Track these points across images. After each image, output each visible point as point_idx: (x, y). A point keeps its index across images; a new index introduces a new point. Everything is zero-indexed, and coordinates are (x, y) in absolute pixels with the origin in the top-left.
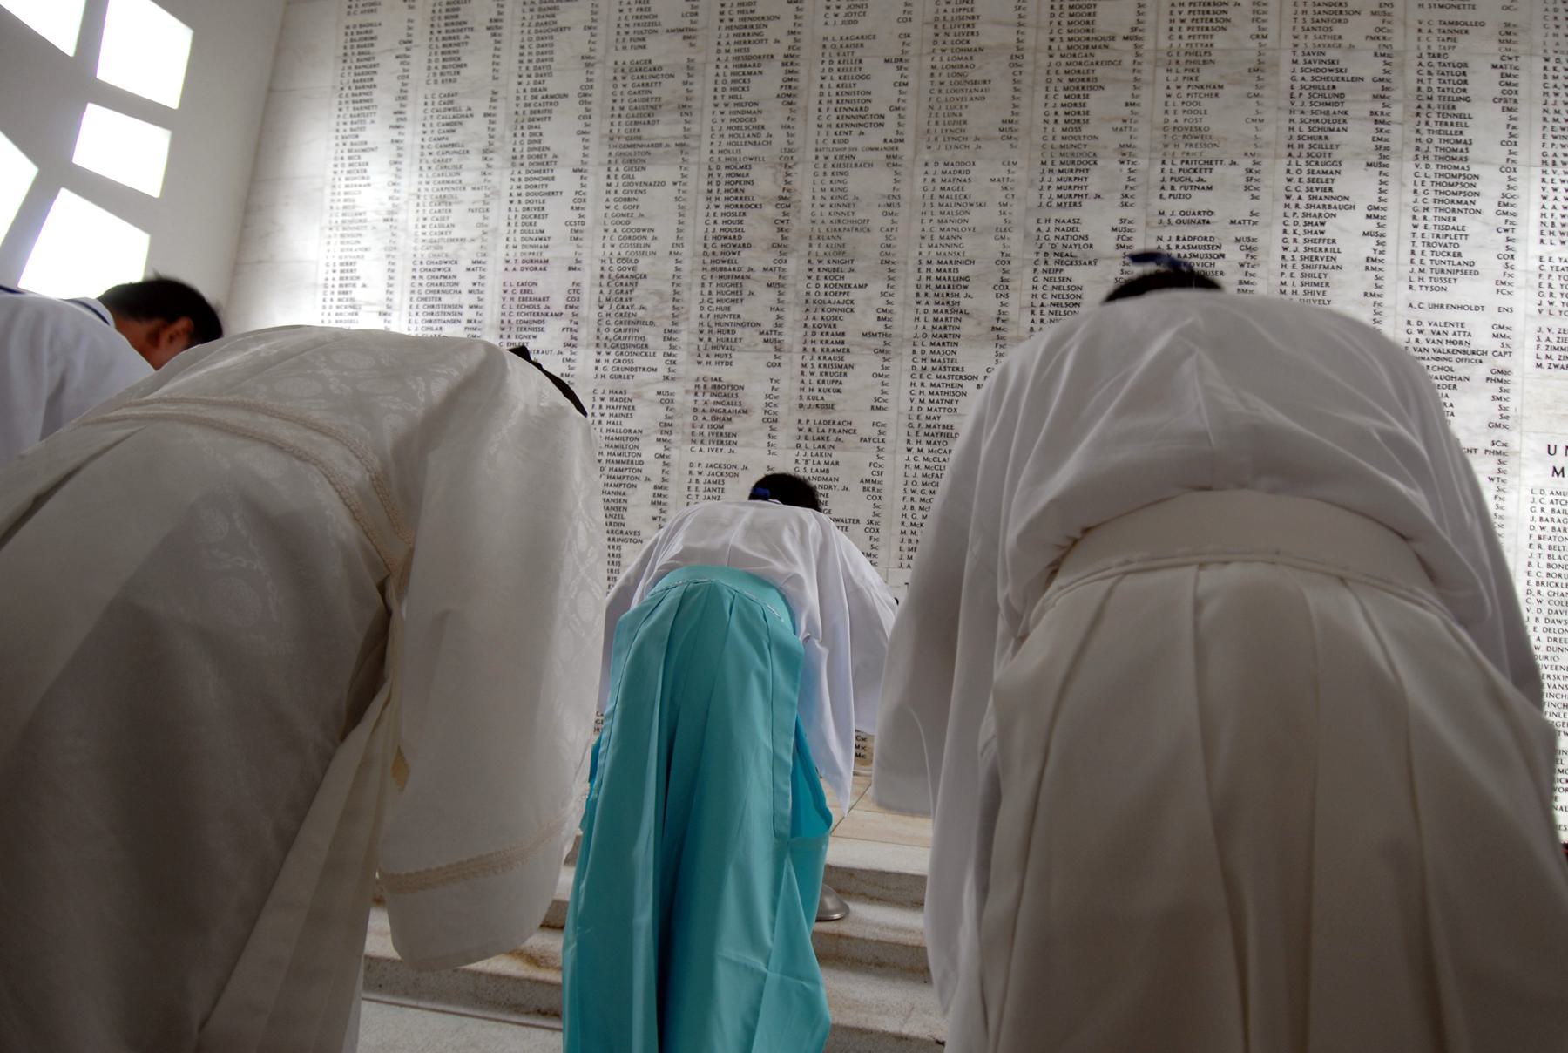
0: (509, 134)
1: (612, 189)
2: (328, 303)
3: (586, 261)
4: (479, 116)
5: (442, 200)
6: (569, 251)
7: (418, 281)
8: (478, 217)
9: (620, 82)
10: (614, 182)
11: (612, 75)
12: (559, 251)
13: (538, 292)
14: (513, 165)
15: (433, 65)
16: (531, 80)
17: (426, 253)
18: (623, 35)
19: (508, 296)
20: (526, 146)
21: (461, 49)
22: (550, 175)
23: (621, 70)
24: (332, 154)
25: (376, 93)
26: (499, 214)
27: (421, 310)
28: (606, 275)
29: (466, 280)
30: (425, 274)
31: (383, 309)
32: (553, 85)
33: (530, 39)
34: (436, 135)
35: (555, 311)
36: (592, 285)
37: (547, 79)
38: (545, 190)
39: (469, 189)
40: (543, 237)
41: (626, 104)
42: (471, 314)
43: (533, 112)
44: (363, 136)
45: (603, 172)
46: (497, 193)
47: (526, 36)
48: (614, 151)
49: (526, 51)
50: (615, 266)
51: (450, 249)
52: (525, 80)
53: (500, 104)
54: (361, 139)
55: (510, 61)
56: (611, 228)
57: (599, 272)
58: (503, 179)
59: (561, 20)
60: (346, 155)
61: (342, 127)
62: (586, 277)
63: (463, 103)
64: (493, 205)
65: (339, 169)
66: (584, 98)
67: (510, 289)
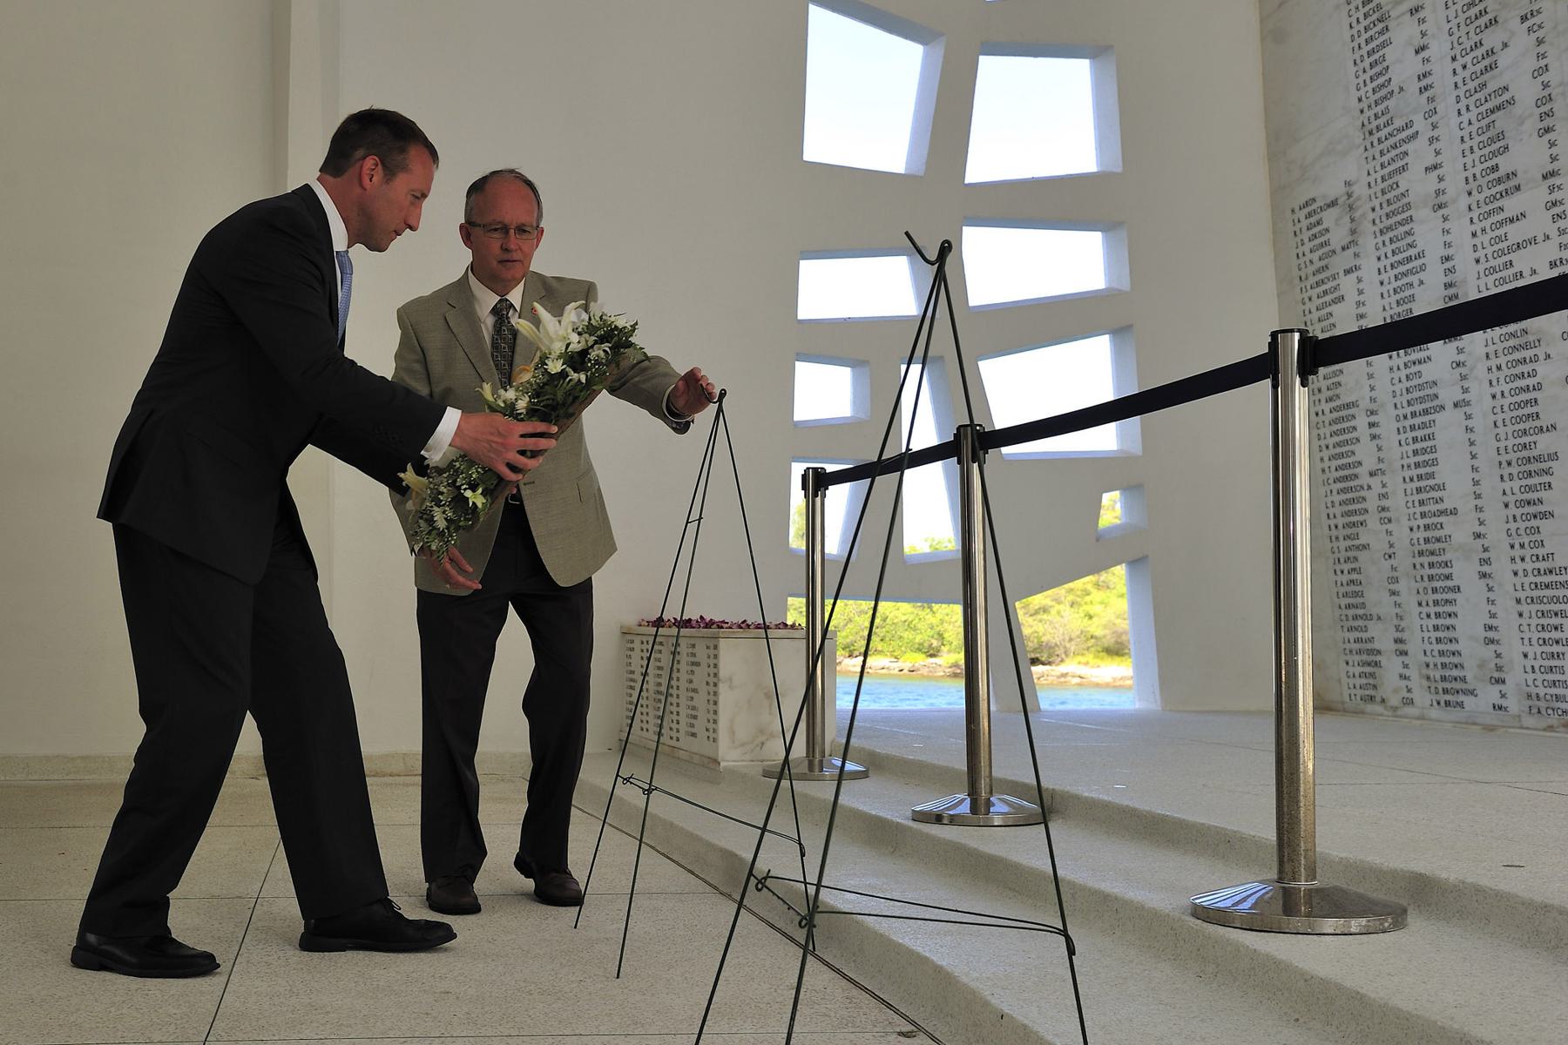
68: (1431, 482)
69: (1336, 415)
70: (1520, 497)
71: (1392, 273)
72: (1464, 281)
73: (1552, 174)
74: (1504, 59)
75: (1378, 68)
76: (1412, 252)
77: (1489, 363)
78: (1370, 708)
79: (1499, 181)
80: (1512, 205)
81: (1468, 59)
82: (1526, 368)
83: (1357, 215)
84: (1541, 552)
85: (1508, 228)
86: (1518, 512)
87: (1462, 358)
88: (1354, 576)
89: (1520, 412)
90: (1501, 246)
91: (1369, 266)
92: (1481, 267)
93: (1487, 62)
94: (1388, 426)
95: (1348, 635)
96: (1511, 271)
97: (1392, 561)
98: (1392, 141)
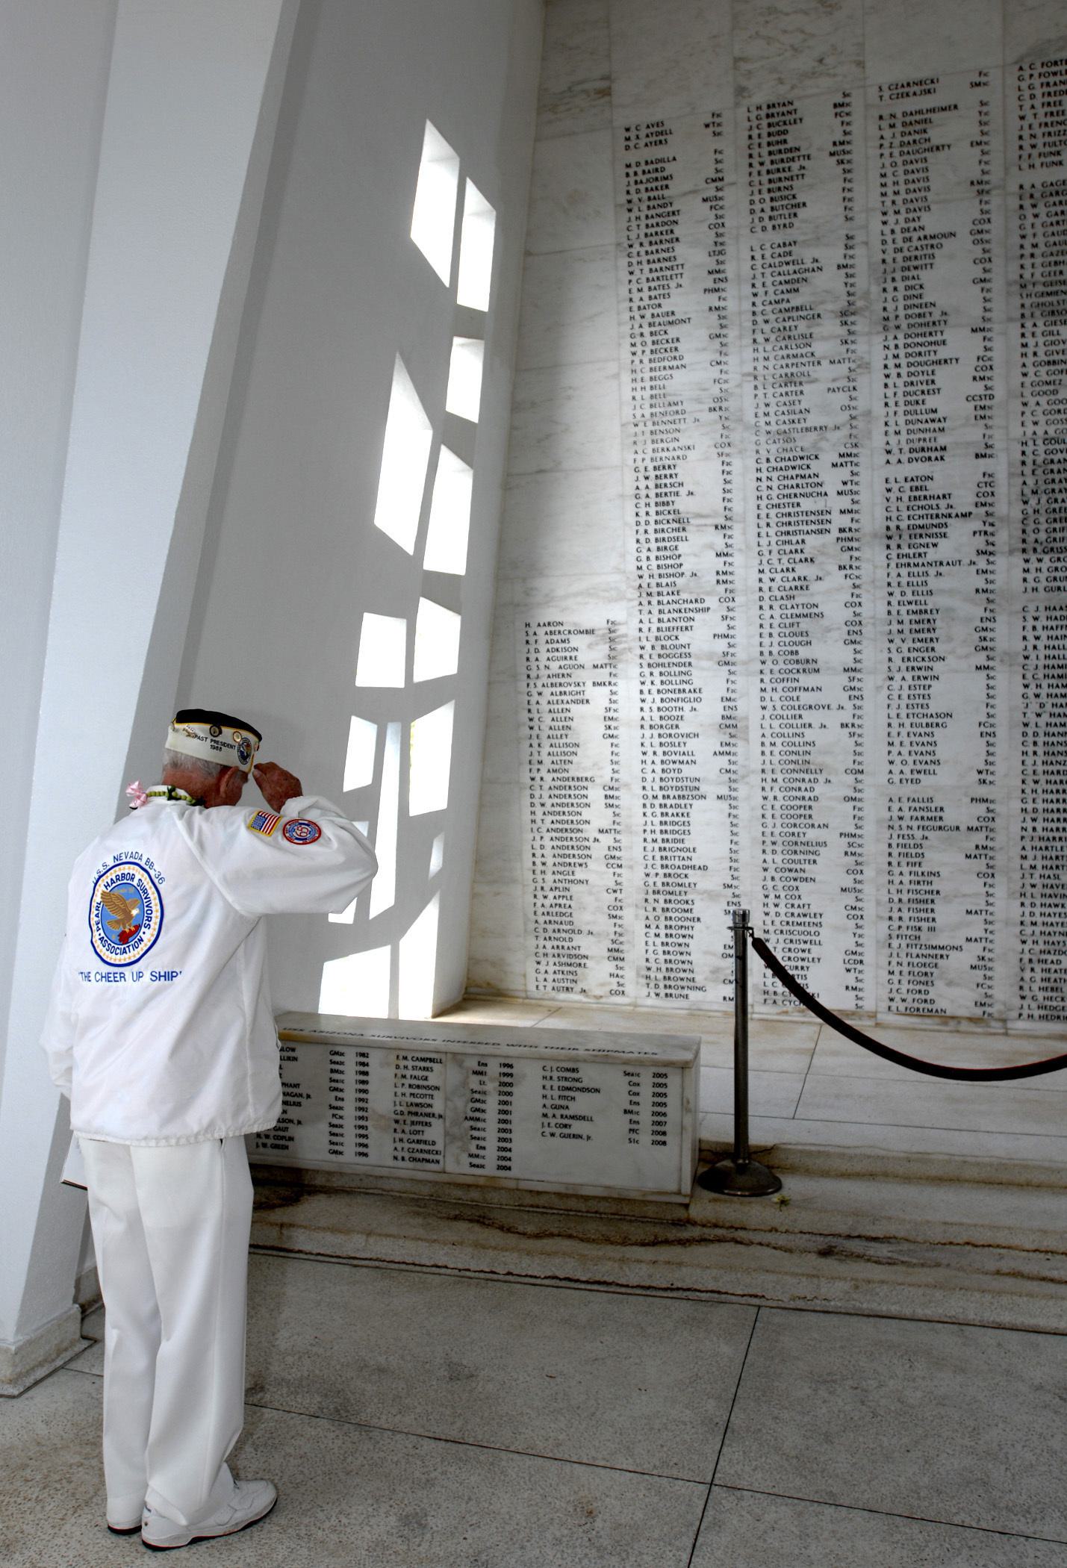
0: (875, 290)
1: (1030, 351)
2: (643, 519)
3: (999, 442)
4: (830, 270)
5: (789, 380)
6: (975, 434)
7: (764, 484)
8: (842, 398)
9: (1029, 212)
10: (1031, 341)
11: (1017, 202)
12: (962, 433)
13: (934, 488)
14: (885, 328)
15: (757, 207)
16: (901, 218)
17: (773, 448)
18: (1028, 149)
19: (893, 496)
20: (901, 304)
21: (795, 183)
22: (939, 338)
23: (1028, 196)
24: (626, 329)
25: (680, 250)
26: (871, 392)
27: (773, 521)
28: (1029, 460)
29: (833, 480)
30: (775, 475)
31: (722, 521)
32: (931, 222)
33: (894, 164)
34: (772, 297)
35: (960, 510)
36: (1011, 475)
37: (924, 215)
38: (933, 357)
39: (825, 363)
40: (935, 418)
41: (1040, 240)
42: (845, 521)
43: (906, 259)
44: (667, 306)
45: (1015, 330)
46: (866, 366)
47: (887, 161)
48: (1028, 302)
49: (889, 180)
50: (1041, 448)
51: (806, 441)
52: (891, 218)
53: (859, 252)
54: (664, 309)
55: (867, 194)
56: (1032, 401)
57: (1020, 458)
58: (873, 348)
59: (936, 136)
60: (646, 330)
61: (636, 296)
62: (1000, 466)
63: (806, 254)
64: (862, 382)
65: (639, 349)
66: (979, 234)
67: (895, 487)
68: (680, 845)
69: (559, 783)
70: (781, 865)
71: (658, 698)
72: (746, 718)
73: (854, 670)
74: (815, 587)
75: (668, 551)
76: (687, 687)
77: (764, 776)
78: (563, 996)
79: (797, 662)
80: (806, 680)
81: (778, 577)
82: (803, 786)
83: (619, 647)
84: (796, 902)
85: (802, 694)
86: (777, 876)
87: (733, 767)
88: (562, 901)
89: (792, 812)
90: (792, 703)
91: (628, 687)
92: (767, 713)
93: (798, 583)
94: (630, 801)
95: (542, 942)
96: (799, 722)
97: (618, 895)
98: (676, 607)
